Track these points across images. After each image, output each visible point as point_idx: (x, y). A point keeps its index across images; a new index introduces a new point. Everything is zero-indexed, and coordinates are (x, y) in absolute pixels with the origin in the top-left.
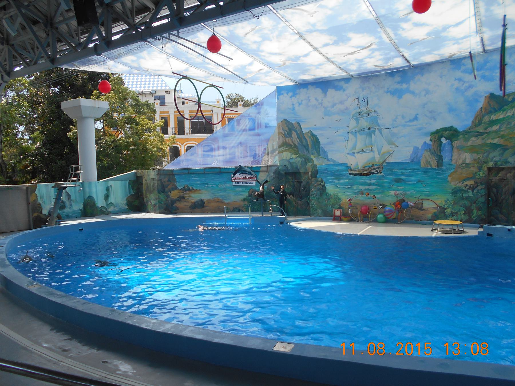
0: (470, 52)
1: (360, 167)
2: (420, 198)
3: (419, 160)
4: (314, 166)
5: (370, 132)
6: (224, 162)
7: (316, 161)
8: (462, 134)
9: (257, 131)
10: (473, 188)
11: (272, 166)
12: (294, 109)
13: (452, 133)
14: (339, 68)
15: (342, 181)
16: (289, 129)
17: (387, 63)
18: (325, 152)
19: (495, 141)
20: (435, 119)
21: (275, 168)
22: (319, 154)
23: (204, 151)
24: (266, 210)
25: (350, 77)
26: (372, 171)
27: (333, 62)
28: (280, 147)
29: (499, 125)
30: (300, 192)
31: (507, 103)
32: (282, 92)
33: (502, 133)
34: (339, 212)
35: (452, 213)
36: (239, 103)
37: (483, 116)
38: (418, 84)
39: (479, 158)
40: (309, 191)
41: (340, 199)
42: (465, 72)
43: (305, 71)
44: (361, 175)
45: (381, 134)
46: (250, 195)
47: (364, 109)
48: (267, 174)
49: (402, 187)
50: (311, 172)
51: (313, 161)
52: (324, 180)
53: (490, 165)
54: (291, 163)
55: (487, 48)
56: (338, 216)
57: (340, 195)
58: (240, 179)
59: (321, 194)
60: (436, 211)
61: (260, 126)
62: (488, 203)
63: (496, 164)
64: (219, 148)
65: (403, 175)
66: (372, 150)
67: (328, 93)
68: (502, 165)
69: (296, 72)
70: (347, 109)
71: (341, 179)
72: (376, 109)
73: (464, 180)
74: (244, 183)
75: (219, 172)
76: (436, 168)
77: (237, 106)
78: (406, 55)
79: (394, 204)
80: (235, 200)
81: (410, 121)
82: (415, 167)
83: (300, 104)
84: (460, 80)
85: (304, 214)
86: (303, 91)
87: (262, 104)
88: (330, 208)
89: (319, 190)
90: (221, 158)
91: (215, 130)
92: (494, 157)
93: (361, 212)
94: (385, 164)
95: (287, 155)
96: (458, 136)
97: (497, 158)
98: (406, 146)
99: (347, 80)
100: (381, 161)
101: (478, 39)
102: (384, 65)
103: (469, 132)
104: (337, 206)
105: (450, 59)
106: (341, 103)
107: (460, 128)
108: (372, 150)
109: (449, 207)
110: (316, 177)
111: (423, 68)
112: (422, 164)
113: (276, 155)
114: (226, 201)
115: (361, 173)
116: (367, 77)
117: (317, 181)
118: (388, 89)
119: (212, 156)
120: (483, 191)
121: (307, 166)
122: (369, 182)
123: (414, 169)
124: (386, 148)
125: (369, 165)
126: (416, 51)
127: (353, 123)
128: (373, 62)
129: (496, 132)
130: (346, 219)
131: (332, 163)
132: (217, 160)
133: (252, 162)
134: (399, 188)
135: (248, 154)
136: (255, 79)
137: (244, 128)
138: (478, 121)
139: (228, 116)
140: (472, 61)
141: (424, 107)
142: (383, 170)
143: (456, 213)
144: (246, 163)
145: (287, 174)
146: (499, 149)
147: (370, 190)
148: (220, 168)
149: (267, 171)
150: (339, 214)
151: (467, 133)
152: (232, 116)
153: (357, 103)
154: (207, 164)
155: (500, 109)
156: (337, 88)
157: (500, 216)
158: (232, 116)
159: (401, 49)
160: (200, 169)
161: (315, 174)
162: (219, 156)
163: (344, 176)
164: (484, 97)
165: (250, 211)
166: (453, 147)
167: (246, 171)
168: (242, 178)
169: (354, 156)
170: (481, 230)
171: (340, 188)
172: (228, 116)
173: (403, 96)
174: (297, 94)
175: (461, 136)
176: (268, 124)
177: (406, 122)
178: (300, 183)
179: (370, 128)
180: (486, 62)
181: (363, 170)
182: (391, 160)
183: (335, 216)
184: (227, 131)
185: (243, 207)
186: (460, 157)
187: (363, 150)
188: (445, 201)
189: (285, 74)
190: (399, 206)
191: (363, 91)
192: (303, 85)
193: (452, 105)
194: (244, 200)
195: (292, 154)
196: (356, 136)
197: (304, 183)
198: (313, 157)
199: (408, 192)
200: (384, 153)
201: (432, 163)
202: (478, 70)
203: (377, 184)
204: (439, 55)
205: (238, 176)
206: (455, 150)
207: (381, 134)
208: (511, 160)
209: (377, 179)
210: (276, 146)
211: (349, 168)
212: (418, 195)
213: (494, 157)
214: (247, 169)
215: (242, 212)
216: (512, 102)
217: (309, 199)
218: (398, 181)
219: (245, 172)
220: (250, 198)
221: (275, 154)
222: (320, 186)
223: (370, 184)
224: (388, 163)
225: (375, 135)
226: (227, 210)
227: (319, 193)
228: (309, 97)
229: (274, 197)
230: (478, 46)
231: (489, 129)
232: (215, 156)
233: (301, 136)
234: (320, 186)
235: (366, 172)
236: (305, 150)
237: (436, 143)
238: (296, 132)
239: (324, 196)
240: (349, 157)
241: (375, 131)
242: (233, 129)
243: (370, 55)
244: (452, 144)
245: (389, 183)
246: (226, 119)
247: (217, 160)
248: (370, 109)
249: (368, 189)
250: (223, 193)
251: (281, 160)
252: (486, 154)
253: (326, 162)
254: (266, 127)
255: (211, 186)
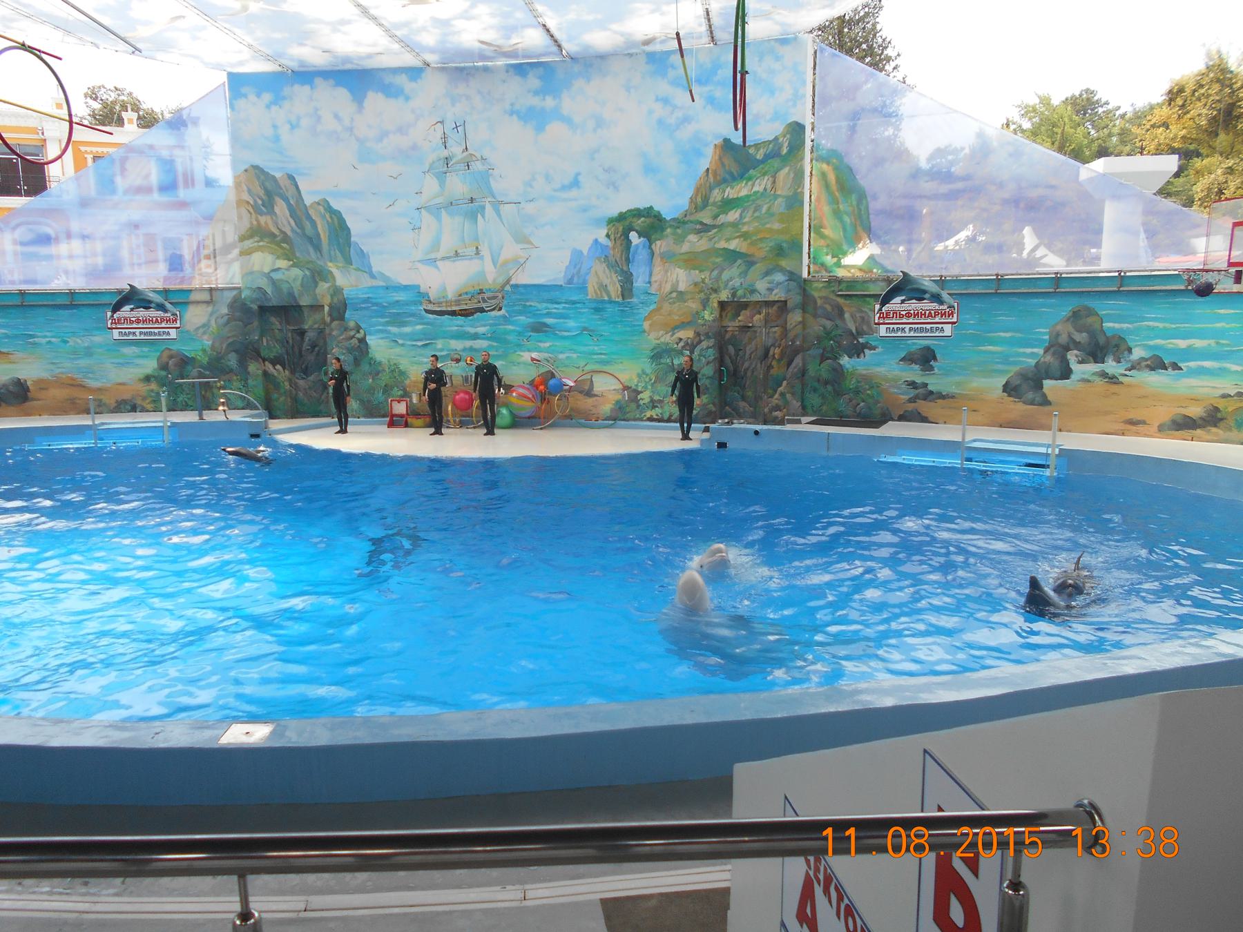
0: (678, 34)
1: (451, 295)
2: (588, 368)
3: (585, 282)
4: (337, 291)
5: (472, 207)
6: (86, 275)
7: (341, 280)
8: (671, 226)
9: (182, 194)
10: (692, 346)
11: (223, 289)
12: (277, 139)
13: (647, 223)
14: (392, 36)
15: (407, 330)
16: (266, 191)
17: (509, 38)
18: (362, 254)
19: (733, 245)
20: (616, 188)
21: (229, 296)
22: (348, 261)
23: (22, 244)
24: (209, 405)
25: (419, 64)
26: (479, 305)
27: (374, 18)
28: (242, 239)
29: (739, 211)
30: (301, 355)
31: (755, 164)
32: (244, 90)
33: (745, 229)
34: (403, 405)
35: (652, 401)
36: (124, 114)
37: (711, 189)
38: (579, 100)
39: (703, 281)
40: (325, 354)
41: (402, 373)
42: (675, 83)
43: (304, 37)
44: (453, 313)
45: (499, 215)
46: (164, 367)
47: (456, 150)
48: (210, 309)
49: (547, 345)
50: (330, 306)
51: (334, 278)
52: (362, 325)
53: (724, 296)
54: (274, 282)
55: (717, 34)
56: (402, 416)
57: (404, 364)
58: (132, 322)
59: (357, 362)
60: (620, 397)
61: (189, 181)
62: (721, 379)
63: (734, 295)
64: (69, 236)
65: (549, 315)
66: (477, 253)
67: (366, 103)
68: (744, 296)
69: (277, 35)
70: (414, 147)
71: (403, 324)
72: (486, 154)
73: (675, 329)
74: (145, 334)
75: (71, 302)
76: (620, 299)
77: (120, 122)
78: (552, 25)
79: (532, 383)
80: (120, 381)
81: (564, 188)
82: (575, 298)
83: (293, 127)
84: (665, 101)
85: (316, 415)
86: (302, 91)
87: (195, 122)
88: (380, 396)
89: (350, 350)
90: (77, 265)
91: (53, 185)
92: (731, 279)
93: (454, 404)
94: (508, 288)
95: (264, 261)
96: (663, 229)
97: (736, 282)
98: (555, 247)
99: (414, 73)
100: (501, 280)
101: (701, 12)
102: (500, 42)
103: (684, 223)
104: (397, 392)
105: (649, 48)
106: (401, 130)
107: (668, 214)
108: (477, 253)
109: (645, 388)
110: (341, 318)
111: (591, 63)
112: (590, 289)
113: (233, 260)
114: (94, 384)
115: (454, 308)
116: (463, 69)
117: (346, 329)
118: (512, 105)
119: (49, 257)
120: (710, 351)
121: (318, 291)
122: (472, 330)
123: (574, 303)
124: (511, 250)
125: (471, 290)
126: (572, 16)
127: (431, 186)
128: (476, 31)
129: (735, 225)
130: (420, 422)
131: (382, 284)
132: (66, 272)
133: (166, 279)
134: (542, 345)
135: (161, 255)
136: (163, 45)
137: (138, 182)
138: (701, 200)
139: (94, 149)
140: (682, 56)
141: (593, 159)
142: (505, 302)
143: (661, 401)
144: (149, 278)
145: (263, 310)
146: (739, 261)
147: (476, 350)
148: (72, 294)
149: (207, 303)
150: (404, 412)
151: (679, 223)
152: (105, 150)
153: (439, 134)
154: (35, 282)
155: (741, 177)
156: (391, 91)
157: (742, 404)
158: (105, 150)
159: (540, 8)
160: (8, 294)
161: (339, 310)
162: (71, 257)
163: (413, 315)
164: (712, 147)
165: (164, 409)
166: (653, 254)
167: (150, 302)
168: (138, 321)
169: (437, 267)
170: (706, 435)
171: (402, 345)
172: (94, 149)
173: (547, 128)
174: (284, 98)
175: (669, 230)
176: (216, 181)
177: (555, 190)
178: (302, 333)
179: (472, 200)
180: (716, 66)
181: (458, 302)
182: (522, 278)
183: (393, 416)
184: (93, 193)
185: (144, 398)
186: (667, 277)
187: (457, 254)
188: (639, 376)
189: (249, 39)
190: (542, 387)
191: (453, 105)
192: (305, 76)
193: (651, 153)
194: (147, 379)
195: (278, 258)
196: (439, 219)
197: (310, 335)
198: (331, 267)
199: (561, 356)
200: (505, 264)
201: (610, 288)
202: (699, 81)
203: (493, 337)
204: (622, 35)
205: (128, 315)
206: (657, 260)
207: (499, 215)
208: (761, 286)
209: (491, 325)
210: (232, 237)
211: (423, 296)
212: (582, 363)
213: (731, 279)
214: (151, 295)
215: (144, 410)
216: (763, 162)
217: (326, 374)
218: (540, 328)
219: (146, 304)
220: (163, 373)
221: (230, 256)
222: (354, 341)
223: (475, 337)
224: (516, 286)
225: (483, 216)
226: (99, 406)
227: (351, 358)
228: (317, 109)
229: (231, 371)
230: (700, 25)
231: (722, 219)
232: (59, 257)
233: (299, 212)
234: (354, 341)
235: (465, 307)
236: (311, 250)
237: (619, 242)
238: (286, 200)
239: (365, 367)
240: (425, 270)
241: (483, 208)
242: (107, 185)
243: (466, 11)
244: (650, 247)
245: (520, 334)
246: (89, 157)
247: (66, 272)
248: (470, 151)
249: (471, 349)
250: (83, 362)
251: (247, 274)
252: (715, 273)
253: (367, 282)
254: (209, 183)
255: (44, 341)
